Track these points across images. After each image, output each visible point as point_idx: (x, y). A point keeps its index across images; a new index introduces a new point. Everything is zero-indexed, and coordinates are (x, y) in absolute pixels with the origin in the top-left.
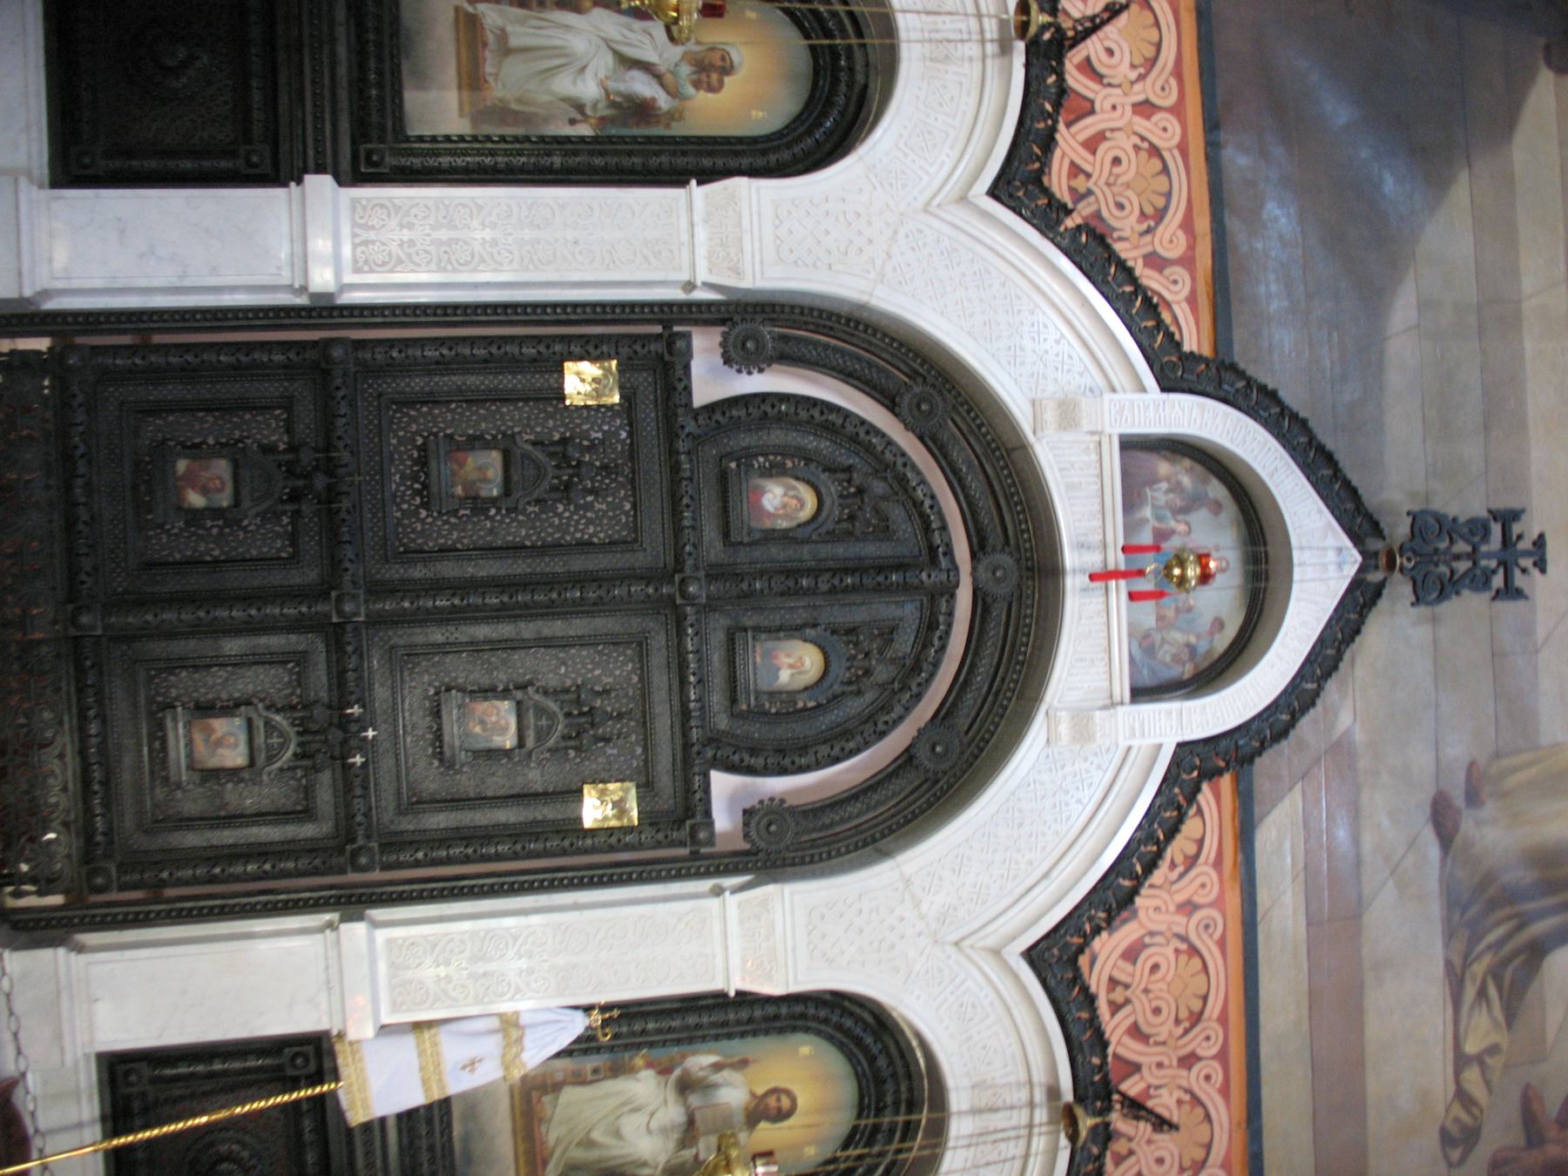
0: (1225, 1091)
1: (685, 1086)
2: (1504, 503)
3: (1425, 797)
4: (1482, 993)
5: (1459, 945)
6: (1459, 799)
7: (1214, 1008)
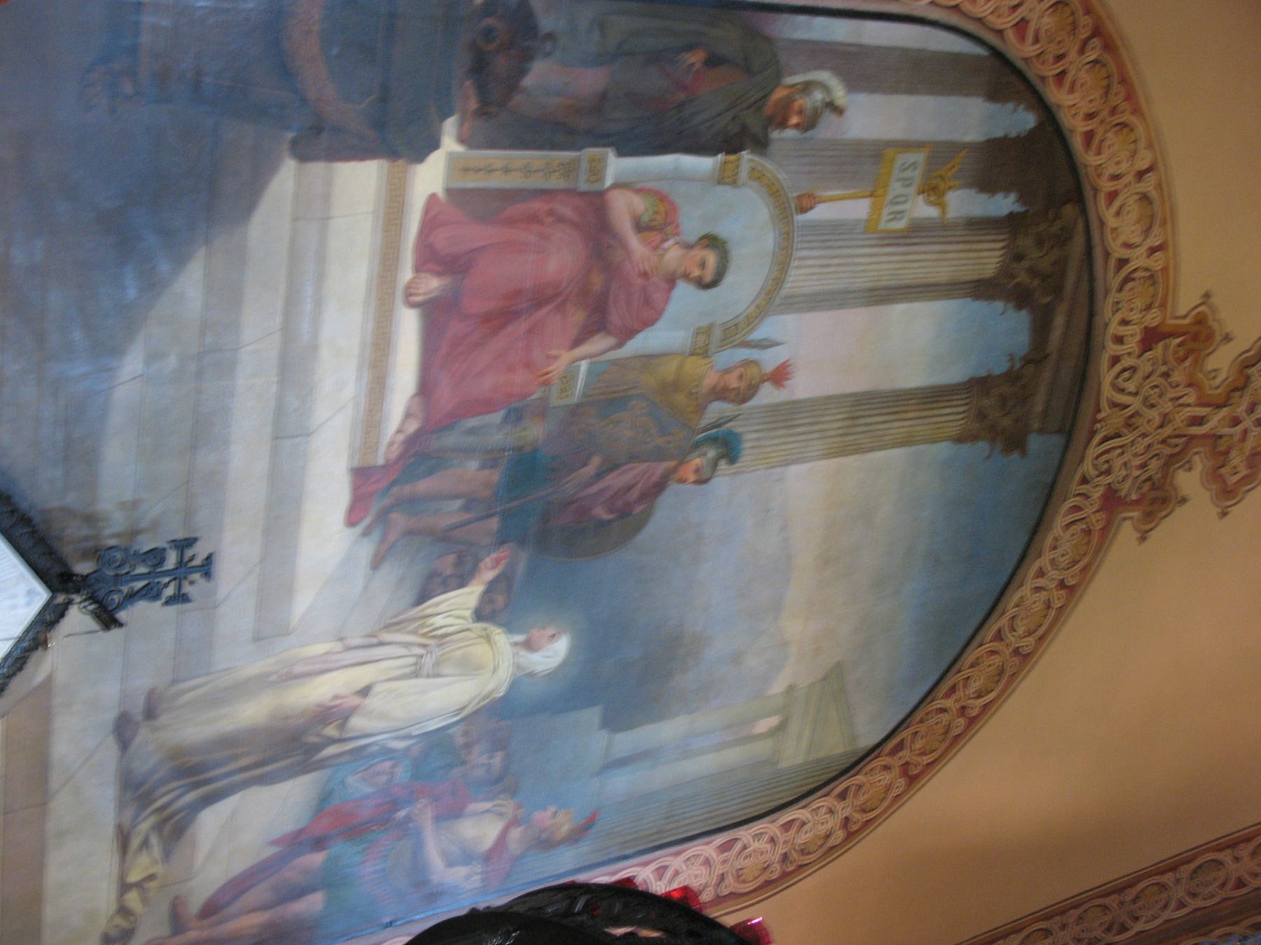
2: (180, 535)
3: (110, 716)
4: (145, 844)
5: (129, 814)
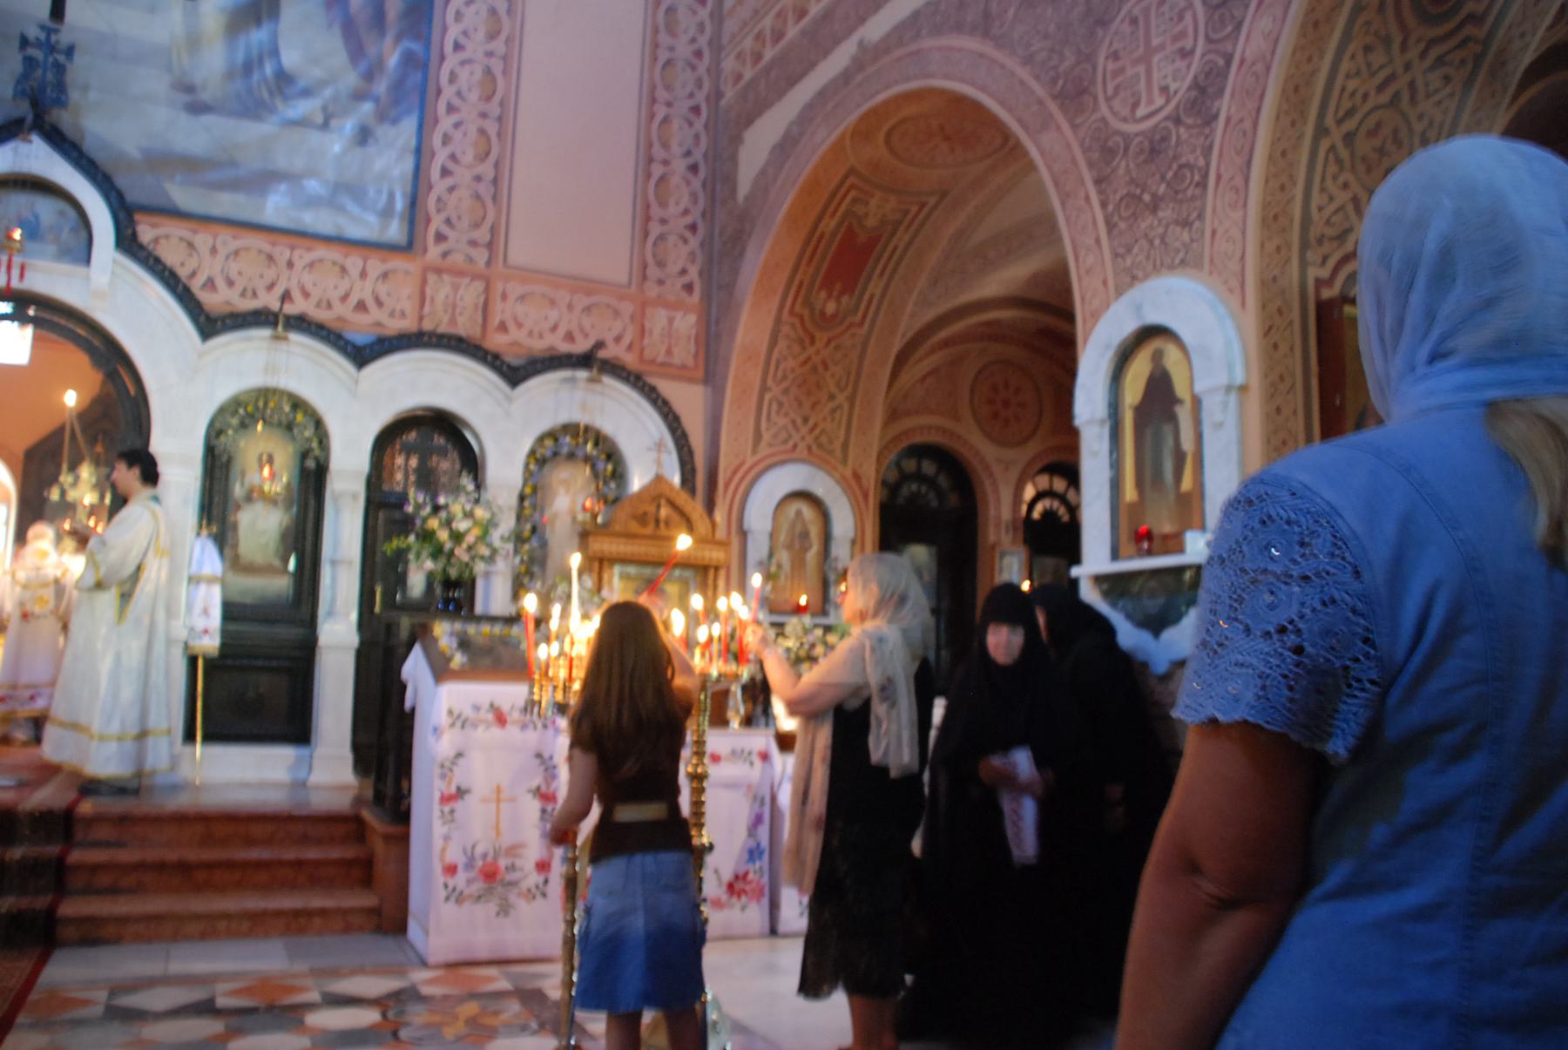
0: (309, 249)
1: (249, 498)
6: (186, 98)
7: (267, 247)
